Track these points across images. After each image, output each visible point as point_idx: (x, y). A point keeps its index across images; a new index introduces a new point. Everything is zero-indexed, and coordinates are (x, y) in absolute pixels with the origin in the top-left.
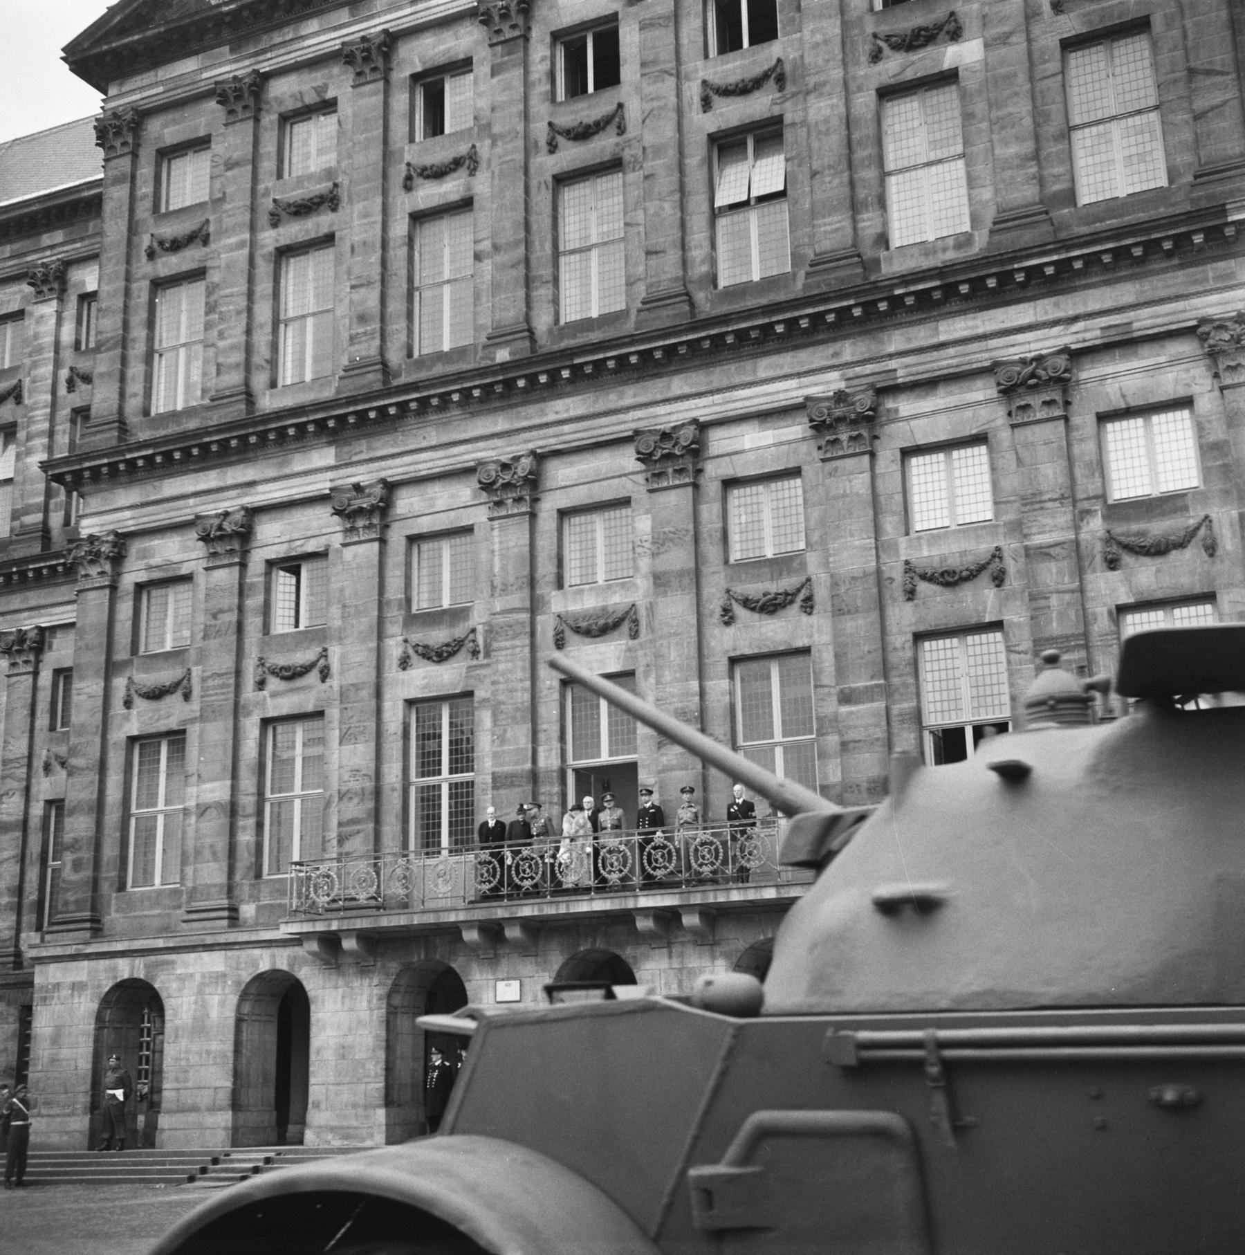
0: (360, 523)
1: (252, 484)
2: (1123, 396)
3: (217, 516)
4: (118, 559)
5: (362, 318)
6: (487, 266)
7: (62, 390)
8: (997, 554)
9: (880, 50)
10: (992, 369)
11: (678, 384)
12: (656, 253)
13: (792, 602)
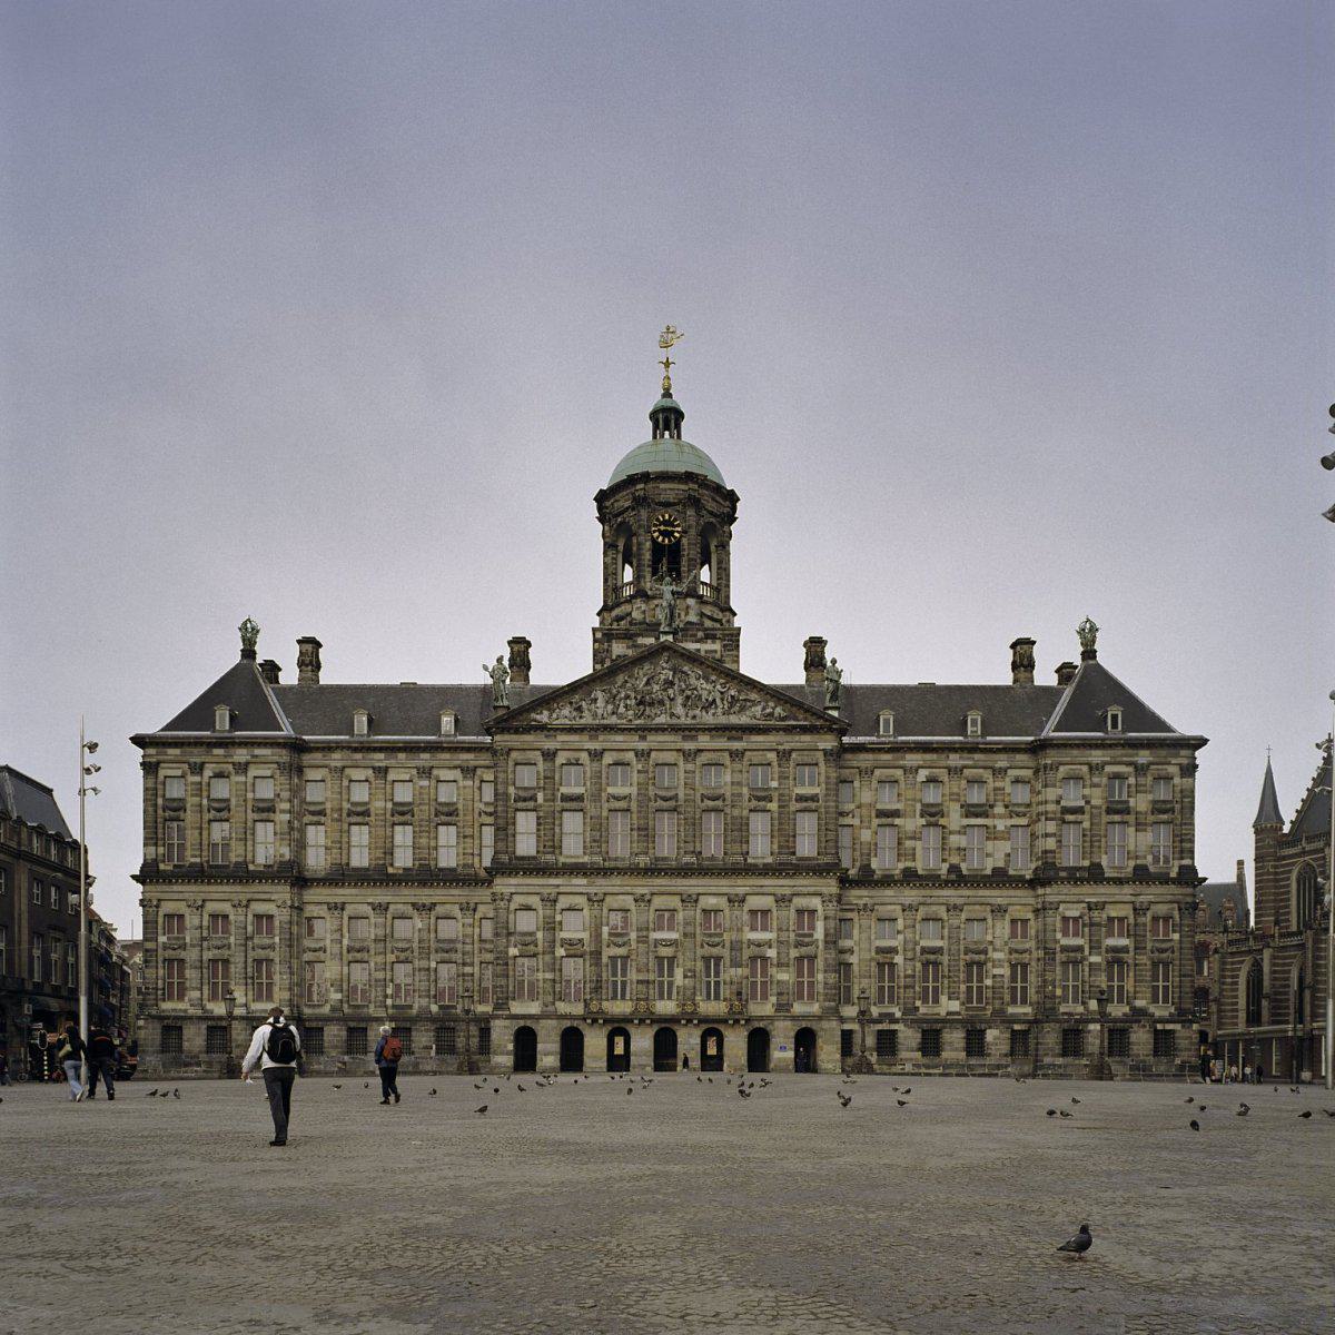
1: (558, 886)
4: (509, 901)
11: (693, 881)
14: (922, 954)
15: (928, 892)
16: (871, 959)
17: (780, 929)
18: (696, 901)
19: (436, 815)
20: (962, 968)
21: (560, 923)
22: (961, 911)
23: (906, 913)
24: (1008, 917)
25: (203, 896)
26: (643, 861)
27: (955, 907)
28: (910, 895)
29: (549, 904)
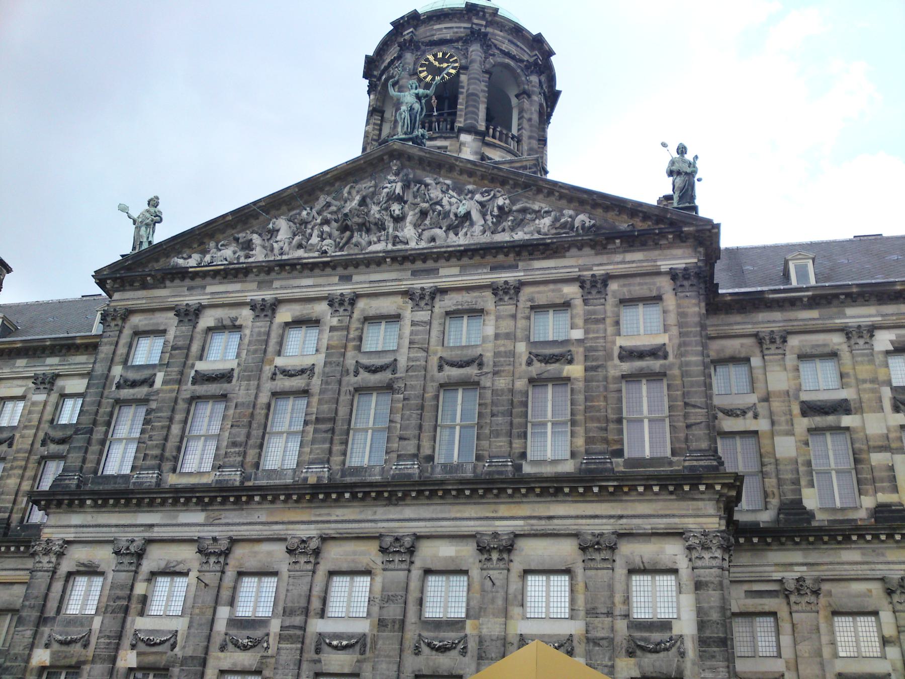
0: (212, 560)
2: (643, 563)
3: (128, 541)
4: (60, 555)
6: (310, 428)
7: (38, 445)
8: (570, 638)
9: (532, 360)
10: (576, 535)
11: (408, 512)
12: (405, 439)
13: (455, 648)
17: (591, 612)
18: (411, 551)
19: (44, 443)
21: (144, 600)
26: (315, 474)
29: (126, 560)
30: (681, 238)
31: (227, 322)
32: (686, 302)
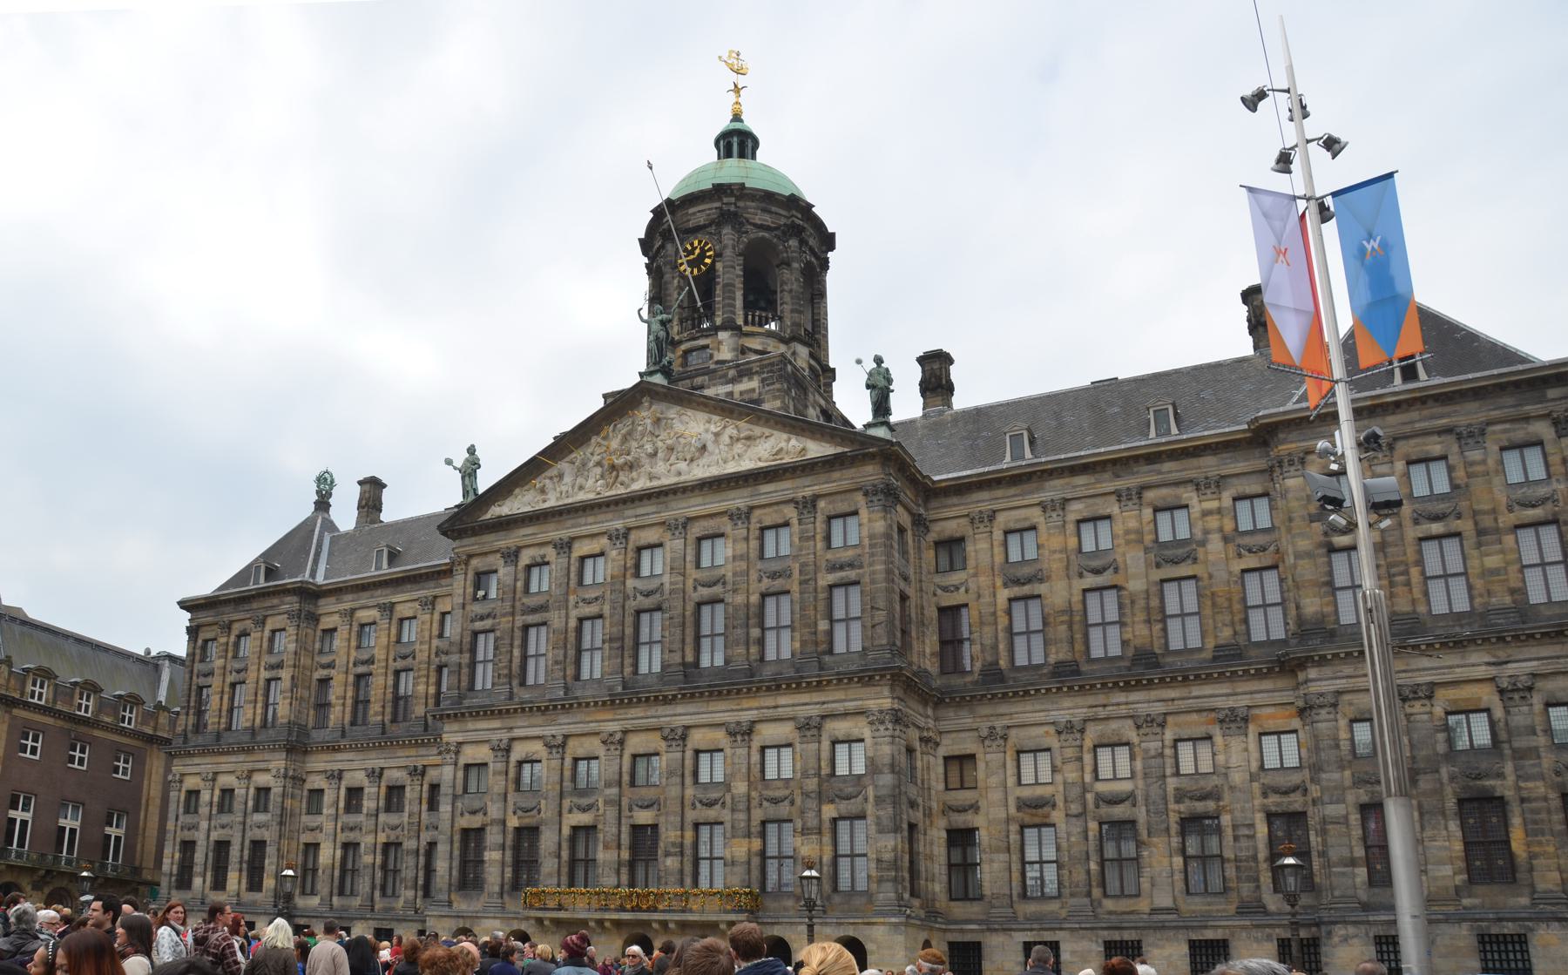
5: (556, 663)
14: (1097, 806)
15: (1101, 699)
16: (1008, 820)
20: (1174, 828)
22: (1162, 725)
23: (1063, 737)
24: (1253, 729)
25: (216, 768)
27: (1150, 720)
28: (1069, 709)
30: (873, 456)
31: (539, 560)
32: (874, 516)
